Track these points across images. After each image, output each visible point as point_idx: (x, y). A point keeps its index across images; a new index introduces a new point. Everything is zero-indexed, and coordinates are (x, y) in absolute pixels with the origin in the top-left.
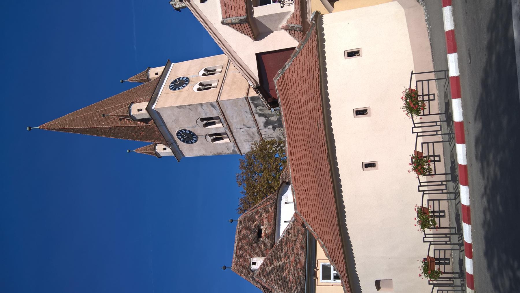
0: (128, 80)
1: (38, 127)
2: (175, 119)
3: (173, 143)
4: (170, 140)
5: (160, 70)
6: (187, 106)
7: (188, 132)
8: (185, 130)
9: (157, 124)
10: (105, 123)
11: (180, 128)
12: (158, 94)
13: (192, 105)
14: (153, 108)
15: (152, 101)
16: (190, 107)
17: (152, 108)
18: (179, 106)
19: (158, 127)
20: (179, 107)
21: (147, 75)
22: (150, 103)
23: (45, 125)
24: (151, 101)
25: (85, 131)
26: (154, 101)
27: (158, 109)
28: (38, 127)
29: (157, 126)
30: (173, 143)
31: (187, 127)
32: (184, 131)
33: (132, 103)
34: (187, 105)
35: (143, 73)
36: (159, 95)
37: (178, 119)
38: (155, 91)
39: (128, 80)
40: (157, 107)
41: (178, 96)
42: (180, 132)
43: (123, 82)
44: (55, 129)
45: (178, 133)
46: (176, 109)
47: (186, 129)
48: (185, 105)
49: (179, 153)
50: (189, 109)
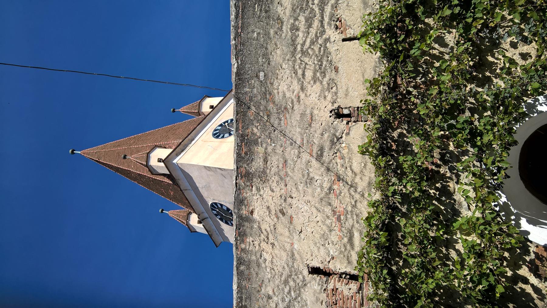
0: (180, 110)
1: (79, 152)
2: (204, 184)
3: (206, 218)
4: (202, 213)
5: (215, 101)
6: (218, 170)
7: (225, 208)
8: (222, 205)
9: (181, 187)
10: (134, 166)
11: (214, 200)
12: (193, 140)
13: (224, 169)
14: (175, 161)
15: (179, 149)
16: (223, 172)
17: (173, 162)
18: (208, 167)
19: (183, 191)
20: (209, 169)
21: (200, 105)
22: (175, 152)
23: (86, 151)
24: (177, 150)
25: (117, 169)
26: (183, 151)
27: (181, 164)
28: (79, 152)
29: (182, 189)
30: (207, 218)
31: (223, 201)
32: (220, 206)
33: (156, 147)
34: (218, 168)
35: (196, 103)
36: (193, 142)
37: (209, 186)
38: (191, 134)
39: (180, 110)
40: (179, 162)
41: (215, 149)
42: (213, 204)
43: (174, 111)
44: (93, 159)
45: (212, 205)
46: (204, 170)
47: (222, 203)
48: (215, 168)
49: (217, 234)
50: (222, 175)
